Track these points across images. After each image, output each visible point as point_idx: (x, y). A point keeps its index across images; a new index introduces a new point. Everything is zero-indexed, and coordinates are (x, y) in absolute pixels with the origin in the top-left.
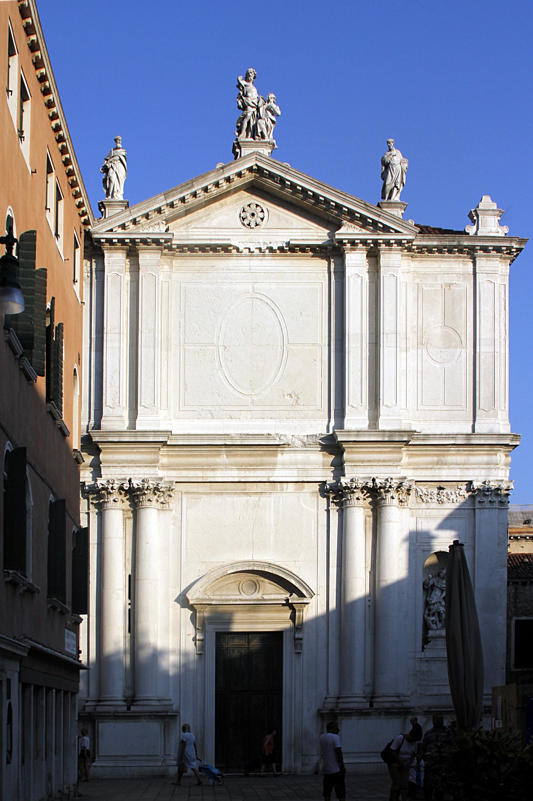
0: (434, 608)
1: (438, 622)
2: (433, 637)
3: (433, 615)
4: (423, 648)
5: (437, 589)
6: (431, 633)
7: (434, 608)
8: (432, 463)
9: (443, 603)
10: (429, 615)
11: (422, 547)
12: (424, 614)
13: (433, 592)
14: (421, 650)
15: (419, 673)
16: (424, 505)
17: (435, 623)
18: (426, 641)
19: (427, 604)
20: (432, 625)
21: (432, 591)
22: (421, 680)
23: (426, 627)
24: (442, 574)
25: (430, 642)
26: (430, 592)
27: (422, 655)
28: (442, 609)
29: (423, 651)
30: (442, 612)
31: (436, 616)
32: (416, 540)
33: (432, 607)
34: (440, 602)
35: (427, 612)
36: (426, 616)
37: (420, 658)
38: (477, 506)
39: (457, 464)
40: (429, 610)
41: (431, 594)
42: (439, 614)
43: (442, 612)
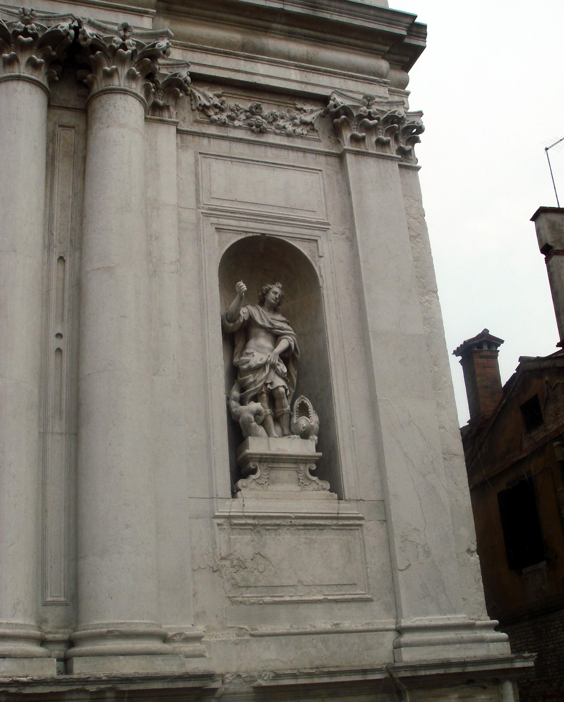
0: (256, 381)
3: (256, 399)
5: (262, 333)
7: (256, 381)
8: (229, 44)
9: (282, 368)
10: (242, 402)
11: (214, 220)
12: (228, 399)
13: (252, 343)
15: (227, 563)
16: (213, 130)
17: (263, 424)
19: (235, 374)
20: (254, 424)
22: (236, 586)
25: (254, 472)
26: (239, 345)
27: (232, 507)
28: (279, 382)
30: (282, 390)
31: (266, 405)
32: (198, 201)
33: (251, 378)
34: (273, 367)
36: (234, 403)
37: (229, 517)
38: (347, 145)
39: (289, 58)
40: (242, 389)
41: (244, 347)
42: (273, 398)
43: (282, 390)
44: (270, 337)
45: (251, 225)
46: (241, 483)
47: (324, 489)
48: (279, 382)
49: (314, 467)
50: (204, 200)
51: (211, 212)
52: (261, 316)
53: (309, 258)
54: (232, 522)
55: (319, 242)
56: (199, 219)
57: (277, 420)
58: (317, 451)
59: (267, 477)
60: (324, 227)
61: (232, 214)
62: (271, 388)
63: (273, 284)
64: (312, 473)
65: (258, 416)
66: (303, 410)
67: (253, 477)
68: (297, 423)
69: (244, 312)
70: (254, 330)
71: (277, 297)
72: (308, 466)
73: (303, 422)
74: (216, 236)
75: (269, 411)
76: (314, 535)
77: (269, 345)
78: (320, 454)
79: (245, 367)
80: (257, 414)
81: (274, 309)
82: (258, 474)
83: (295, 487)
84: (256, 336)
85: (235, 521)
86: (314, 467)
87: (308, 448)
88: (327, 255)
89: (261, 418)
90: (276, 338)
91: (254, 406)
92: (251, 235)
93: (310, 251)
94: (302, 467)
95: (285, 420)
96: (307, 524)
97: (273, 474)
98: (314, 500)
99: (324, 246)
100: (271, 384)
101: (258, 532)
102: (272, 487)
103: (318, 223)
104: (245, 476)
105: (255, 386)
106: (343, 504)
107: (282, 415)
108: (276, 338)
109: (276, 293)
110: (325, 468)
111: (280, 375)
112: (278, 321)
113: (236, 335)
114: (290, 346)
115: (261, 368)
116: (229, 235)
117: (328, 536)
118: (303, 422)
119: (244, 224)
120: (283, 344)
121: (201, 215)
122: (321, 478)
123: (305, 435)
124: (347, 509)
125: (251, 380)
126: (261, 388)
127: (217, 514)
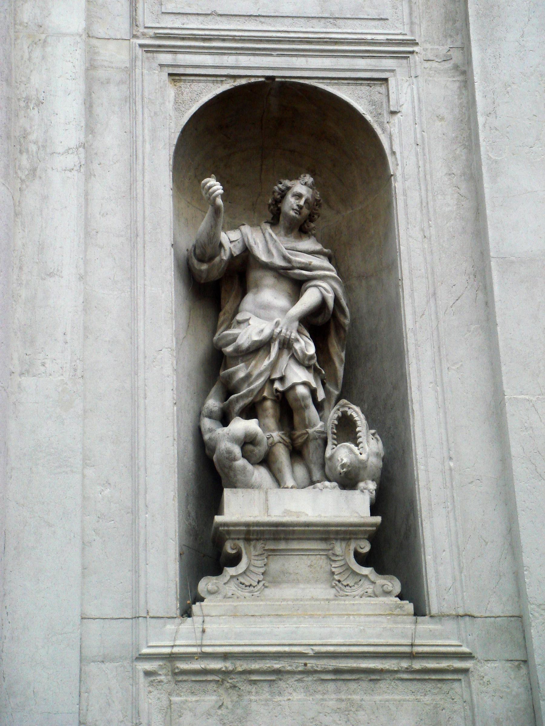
1: (282, 455)
2: (254, 533)
3: (251, 411)
4: (189, 602)
5: (269, 279)
6: (238, 508)
9: (307, 346)
11: (166, 58)
12: (199, 415)
13: (249, 301)
14: (173, 605)
17: (267, 461)
18: (209, 552)
19: (215, 364)
20: (241, 462)
21: (244, 292)
23: (209, 478)
24: (291, 202)
25: (235, 560)
26: (228, 307)
27: (181, 637)
29: (187, 613)
30: (302, 390)
31: (271, 422)
32: (134, 21)
34: (286, 345)
35: (213, 403)
36: (207, 423)
37: (171, 657)
42: (287, 409)
43: (302, 390)
44: (285, 286)
45: (244, 60)
46: (206, 584)
47: (387, 593)
48: (298, 375)
49: (366, 547)
50: (147, 18)
51: (161, 43)
52: (265, 243)
53: (368, 117)
54: (177, 670)
55: (392, 82)
56: (133, 60)
57: (296, 453)
58: (373, 513)
59: (262, 570)
60: (402, 50)
61: (205, 42)
62: (280, 388)
63: (295, 177)
64: (363, 560)
65: (250, 447)
66: (346, 429)
67: (230, 571)
68: (332, 457)
69: (230, 240)
70: (255, 275)
71: (302, 203)
72: (353, 546)
73: (343, 454)
74: (171, 91)
75: (276, 435)
76: (358, 693)
77: (282, 301)
78: (378, 519)
79: (229, 349)
80: (248, 442)
81: (301, 228)
82: (242, 566)
83: (321, 591)
84: (258, 286)
85: (183, 666)
86: (366, 547)
87: (354, 507)
88: (406, 109)
89: (260, 451)
90: (298, 286)
91: (240, 426)
92: (243, 82)
93: (372, 103)
94: (339, 548)
95: (312, 451)
96: (343, 669)
97: (277, 565)
98: (361, 616)
99: (403, 90)
100: (282, 379)
101: (234, 687)
102: (272, 592)
103: (389, 42)
104: (217, 571)
105: (249, 385)
106: (425, 625)
107: (306, 443)
108: (298, 286)
109: (299, 196)
110: (388, 547)
111: (302, 362)
112: (305, 252)
113: (214, 285)
114: (323, 302)
115: (260, 348)
116: (196, 87)
117: (388, 694)
118: (343, 454)
119: (230, 60)
120: (310, 298)
121: (139, 51)
122: (381, 570)
123: (348, 481)
124: (432, 635)
125: (242, 374)
126: (262, 390)
127: (145, 651)
